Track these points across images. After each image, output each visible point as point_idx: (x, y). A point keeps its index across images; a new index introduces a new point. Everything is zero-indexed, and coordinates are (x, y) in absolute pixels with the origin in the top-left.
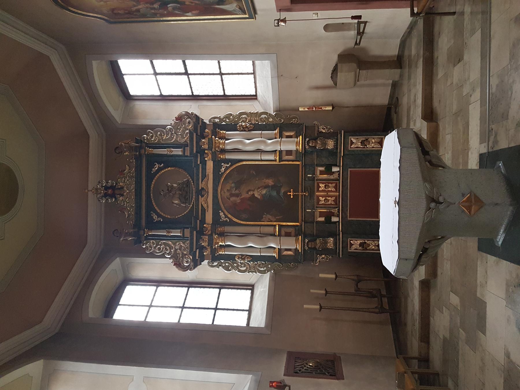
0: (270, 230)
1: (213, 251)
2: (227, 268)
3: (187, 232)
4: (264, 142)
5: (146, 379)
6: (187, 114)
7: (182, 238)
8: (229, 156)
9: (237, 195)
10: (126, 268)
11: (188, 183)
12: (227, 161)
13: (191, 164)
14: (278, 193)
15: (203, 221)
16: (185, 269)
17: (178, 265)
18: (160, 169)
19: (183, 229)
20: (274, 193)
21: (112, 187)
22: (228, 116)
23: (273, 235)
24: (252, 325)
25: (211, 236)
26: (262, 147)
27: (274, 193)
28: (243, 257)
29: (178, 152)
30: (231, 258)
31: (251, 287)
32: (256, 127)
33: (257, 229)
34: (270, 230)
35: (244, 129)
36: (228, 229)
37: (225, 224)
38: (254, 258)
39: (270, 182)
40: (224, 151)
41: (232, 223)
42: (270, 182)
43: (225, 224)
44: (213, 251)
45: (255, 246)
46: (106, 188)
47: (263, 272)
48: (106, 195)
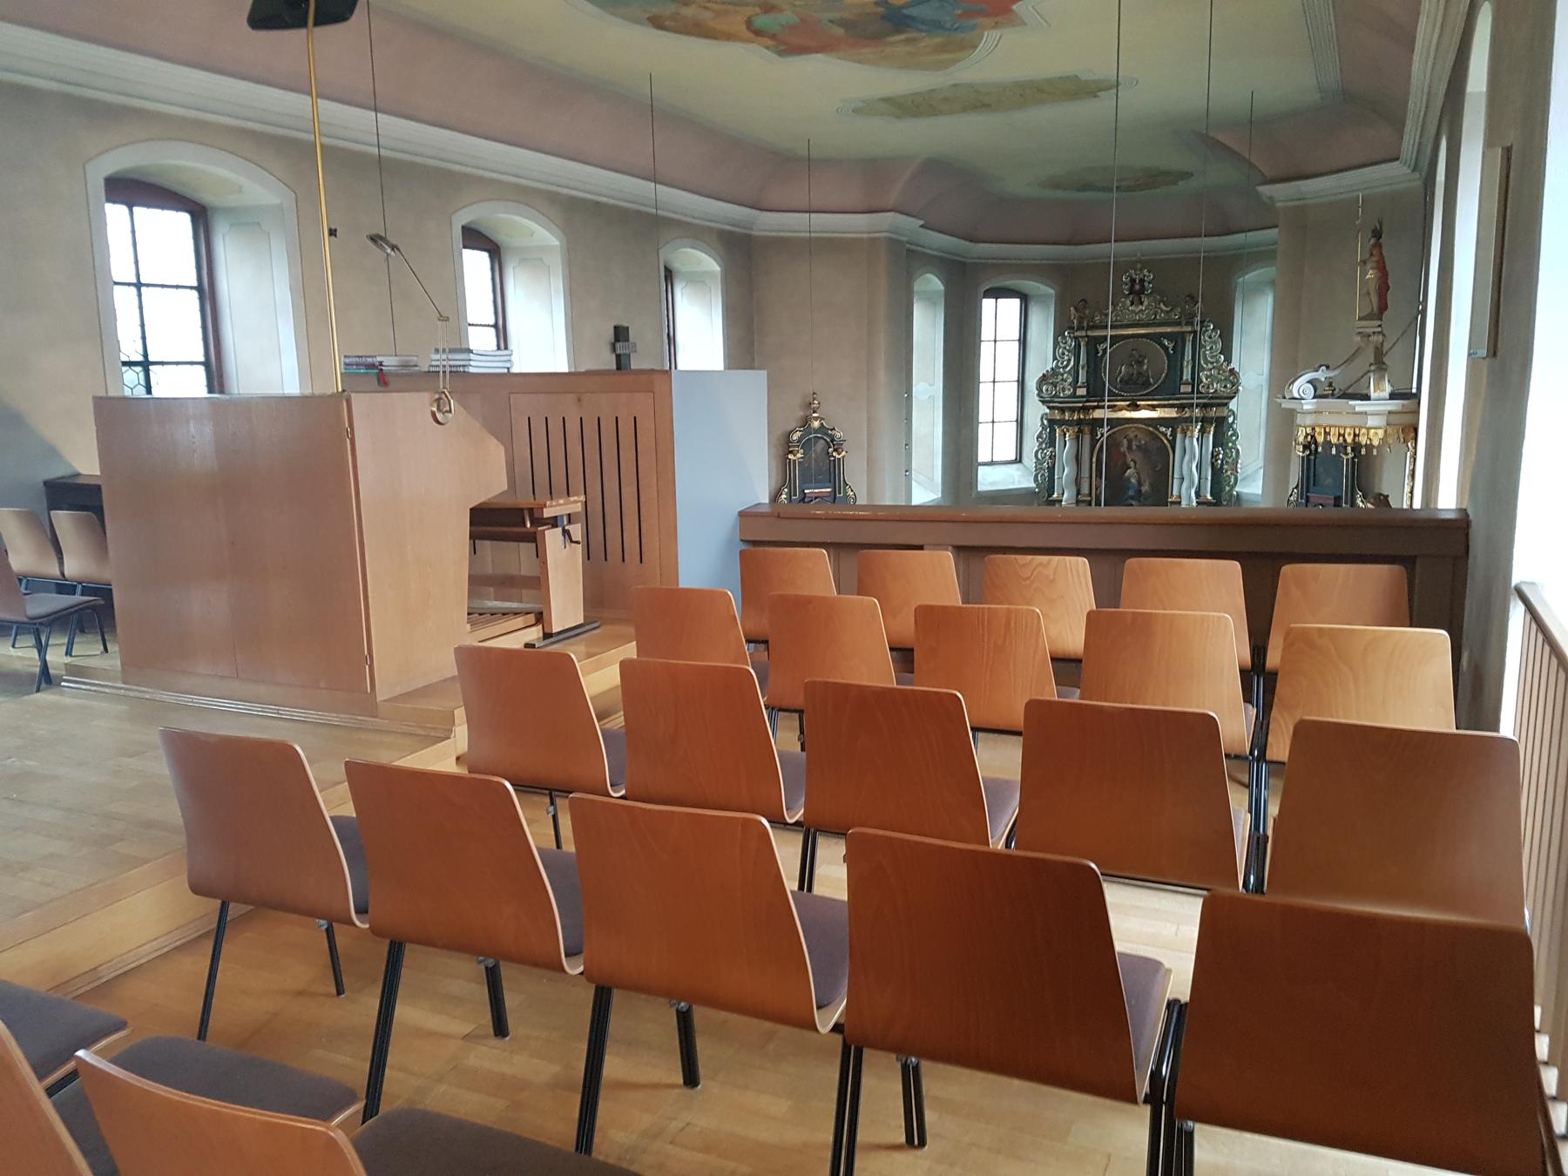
0: (1085, 490)
1: (1061, 423)
2: (1039, 436)
3: (1082, 392)
4: (1190, 487)
5: (932, 398)
6: (1235, 384)
7: (1075, 384)
8: (1179, 436)
9: (1130, 447)
10: (1042, 299)
11: (1147, 384)
12: (1174, 434)
13: (1167, 390)
14: (1132, 498)
15: (1095, 408)
16: (1040, 390)
17: (1044, 379)
18: (1166, 349)
19: (1088, 385)
20: (1131, 493)
21: (1143, 289)
22: (1235, 434)
23: (1078, 493)
24: (981, 468)
25: (1079, 422)
26: (1185, 485)
27: (1131, 493)
28: (1052, 457)
29: (1187, 375)
30: (1052, 443)
31: (1019, 460)
32: (1217, 473)
33: (1085, 474)
34: (1085, 490)
35: (1214, 456)
36: (1087, 438)
37: (1093, 433)
38: (1051, 469)
39: (1145, 488)
40: (1184, 433)
41: (1094, 441)
42: (1145, 488)
43: (1093, 433)
44: (1061, 423)
45: (1065, 474)
46: (1142, 281)
47: (1036, 480)
48: (1133, 281)
